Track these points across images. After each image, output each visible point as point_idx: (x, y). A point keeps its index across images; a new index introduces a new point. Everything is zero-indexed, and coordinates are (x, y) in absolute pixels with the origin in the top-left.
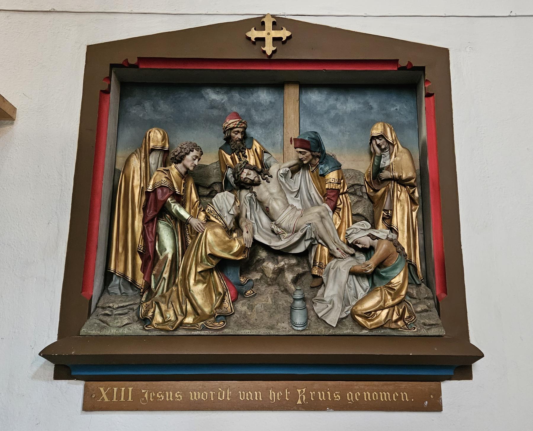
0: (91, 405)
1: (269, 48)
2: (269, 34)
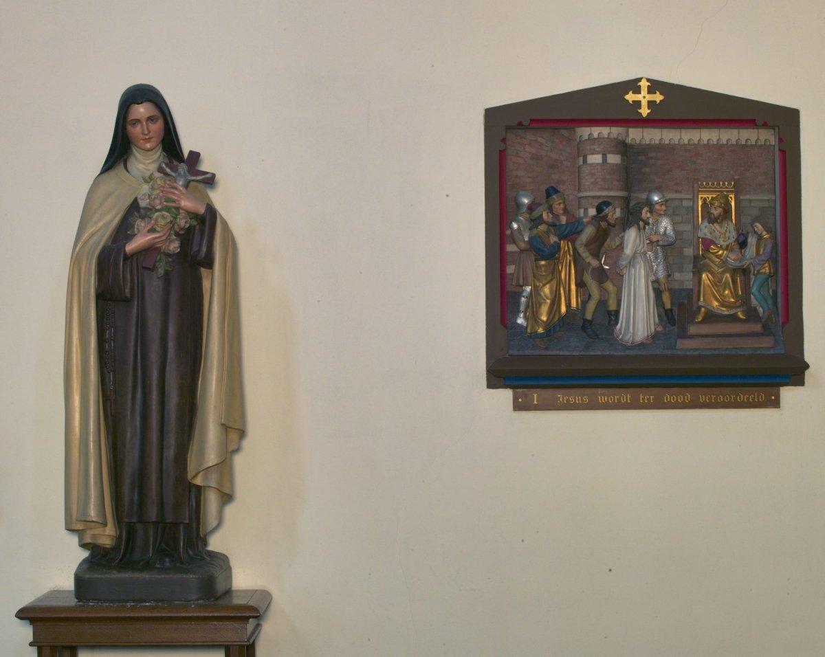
0: (518, 407)
1: (645, 111)
2: (644, 97)
